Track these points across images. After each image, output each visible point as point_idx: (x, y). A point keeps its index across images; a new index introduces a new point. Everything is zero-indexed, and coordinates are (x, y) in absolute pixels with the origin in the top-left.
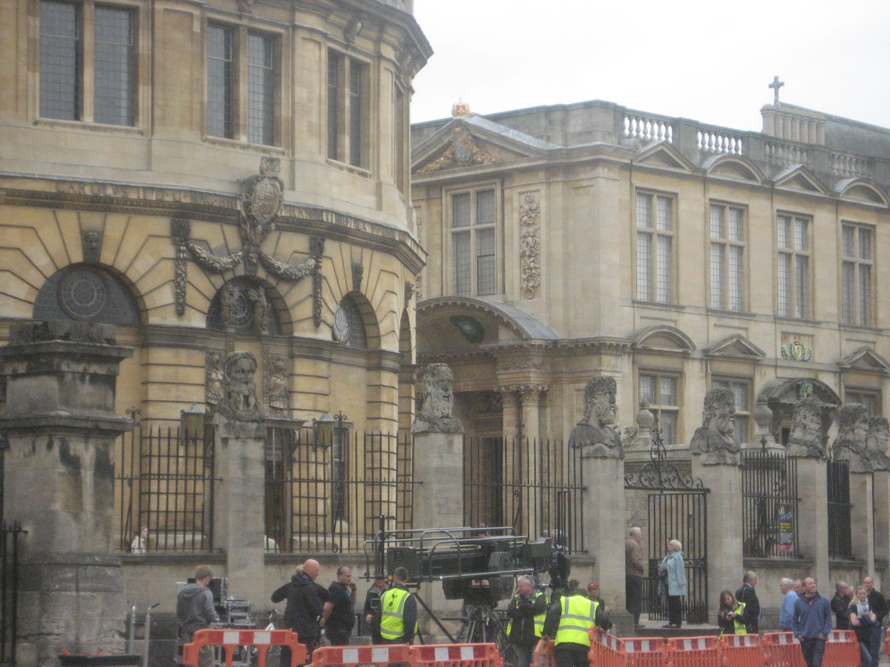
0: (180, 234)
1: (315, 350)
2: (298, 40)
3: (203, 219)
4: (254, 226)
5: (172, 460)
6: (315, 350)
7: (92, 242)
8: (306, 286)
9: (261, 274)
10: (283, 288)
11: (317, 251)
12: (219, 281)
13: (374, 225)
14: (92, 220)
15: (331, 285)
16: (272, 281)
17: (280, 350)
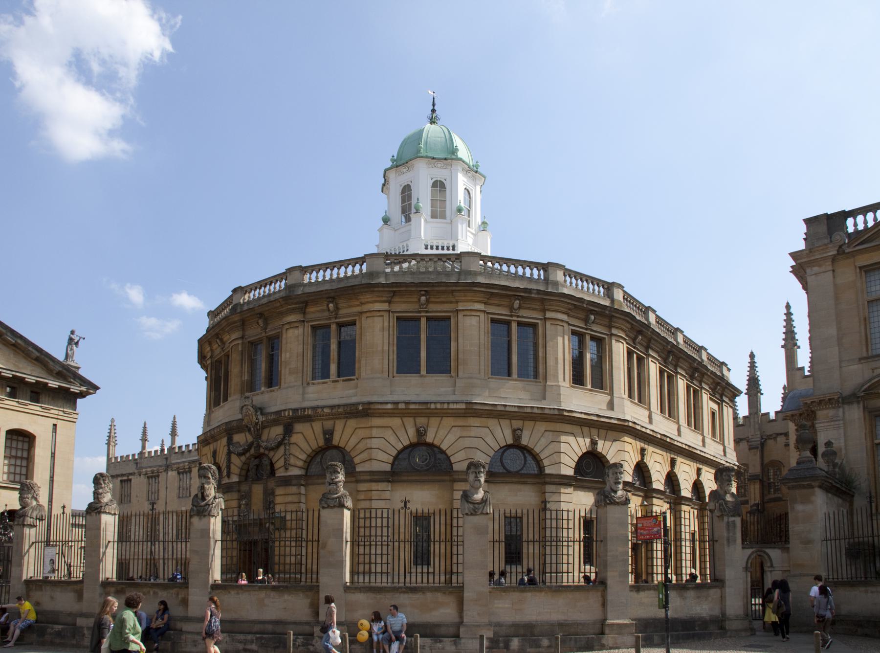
0: (230, 441)
1: (287, 481)
2: (284, 331)
3: (237, 433)
4: (249, 430)
5: (310, 544)
6: (287, 481)
7: (214, 454)
8: (282, 449)
9: (262, 450)
10: (271, 454)
11: (289, 430)
12: (243, 458)
13: (332, 407)
14: (215, 444)
15: (302, 446)
16: (266, 452)
17: (271, 484)
